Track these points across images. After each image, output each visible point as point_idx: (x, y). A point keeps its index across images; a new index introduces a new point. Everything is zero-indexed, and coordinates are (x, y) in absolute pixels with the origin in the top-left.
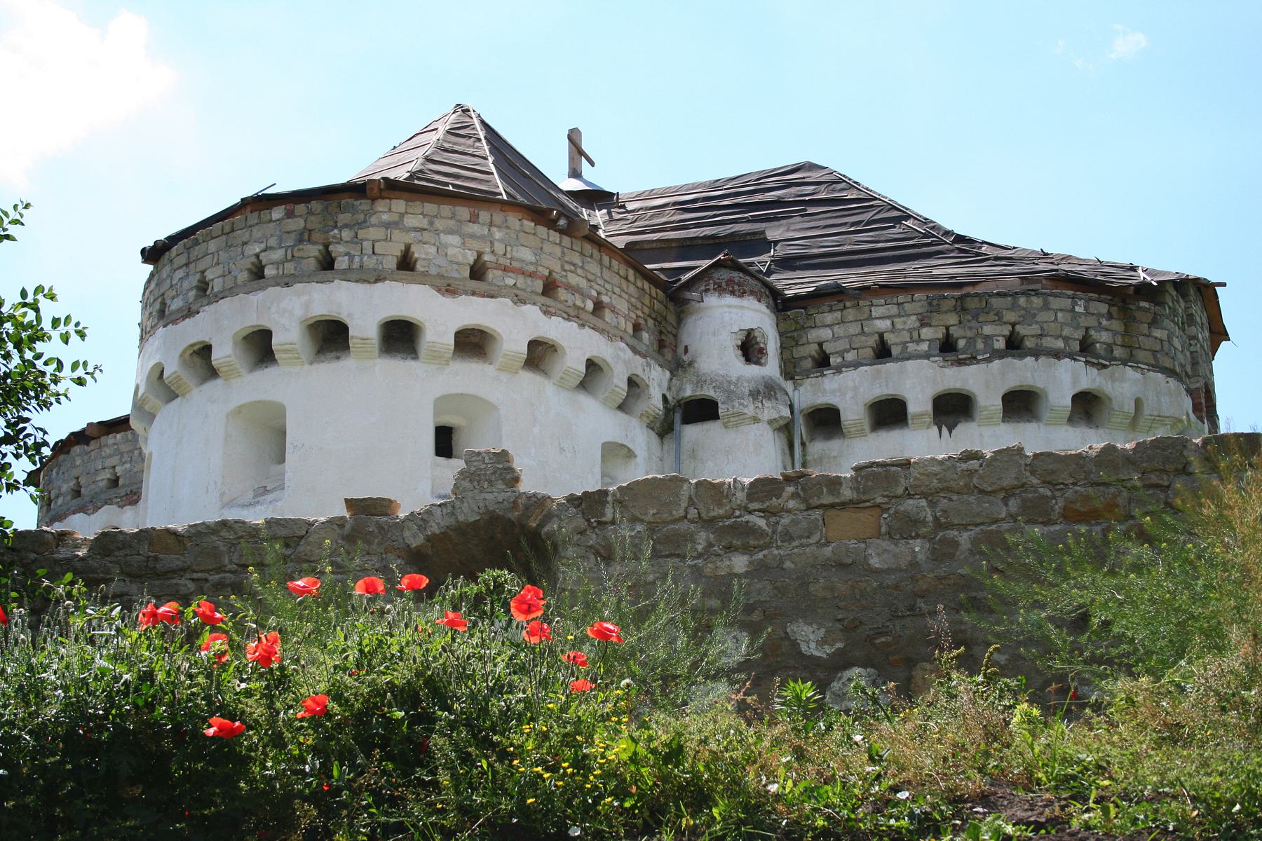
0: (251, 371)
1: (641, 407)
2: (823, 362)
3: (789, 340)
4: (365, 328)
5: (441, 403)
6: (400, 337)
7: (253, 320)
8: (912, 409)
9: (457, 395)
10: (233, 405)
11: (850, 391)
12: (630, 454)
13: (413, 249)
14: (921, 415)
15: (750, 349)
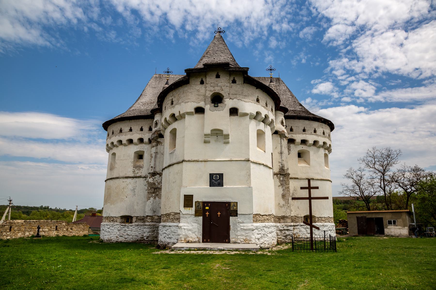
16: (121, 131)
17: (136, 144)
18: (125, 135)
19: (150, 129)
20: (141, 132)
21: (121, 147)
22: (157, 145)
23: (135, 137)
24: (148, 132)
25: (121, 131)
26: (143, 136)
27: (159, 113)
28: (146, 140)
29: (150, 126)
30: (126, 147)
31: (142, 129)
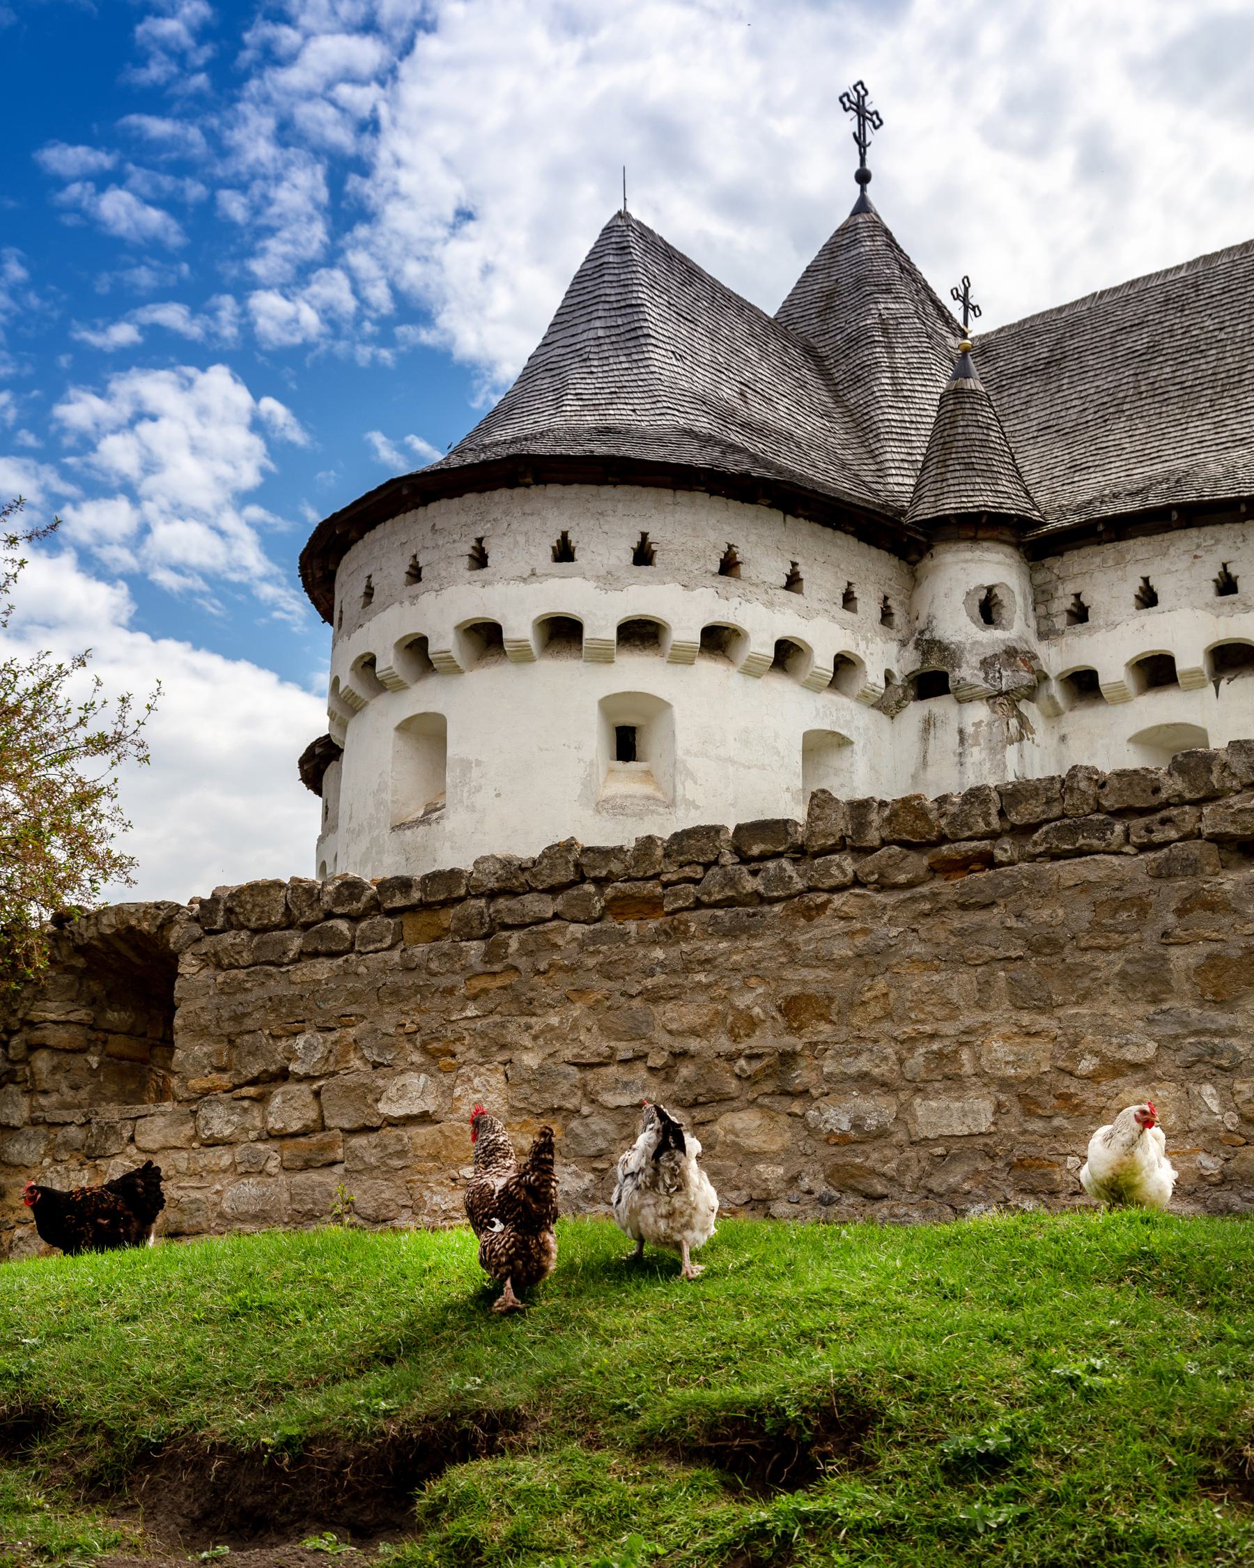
0: (417, 680)
1: (858, 686)
2: (1080, 614)
3: (1041, 596)
4: (520, 629)
5: (608, 705)
6: (562, 632)
7: (411, 628)
8: (1181, 666)
9: (624, 693)
10: (398, 721)
11: (1111, 649)
12: (842, 742)
13: (570, 537)
14: (1194, 672)
15: (989, 609)
16: (729, 566)
17: (813, 686)
18: (770, 604)
19: (886, 616)
20: (847, 615)
21: (709, 670)
22: (1021, 739)
23: (825, 637)
24: (878, 626)
25: (729, 566)
26: (863, 644)
27: (1009, 550)
28: (873, 676)
29: (886, 598)
30: (755, 685)
31: (848, 600)
